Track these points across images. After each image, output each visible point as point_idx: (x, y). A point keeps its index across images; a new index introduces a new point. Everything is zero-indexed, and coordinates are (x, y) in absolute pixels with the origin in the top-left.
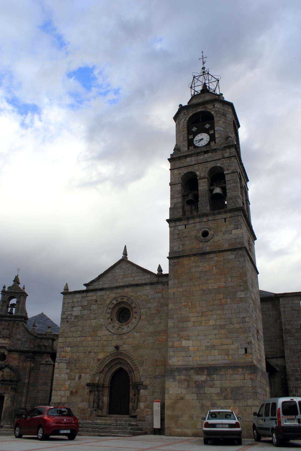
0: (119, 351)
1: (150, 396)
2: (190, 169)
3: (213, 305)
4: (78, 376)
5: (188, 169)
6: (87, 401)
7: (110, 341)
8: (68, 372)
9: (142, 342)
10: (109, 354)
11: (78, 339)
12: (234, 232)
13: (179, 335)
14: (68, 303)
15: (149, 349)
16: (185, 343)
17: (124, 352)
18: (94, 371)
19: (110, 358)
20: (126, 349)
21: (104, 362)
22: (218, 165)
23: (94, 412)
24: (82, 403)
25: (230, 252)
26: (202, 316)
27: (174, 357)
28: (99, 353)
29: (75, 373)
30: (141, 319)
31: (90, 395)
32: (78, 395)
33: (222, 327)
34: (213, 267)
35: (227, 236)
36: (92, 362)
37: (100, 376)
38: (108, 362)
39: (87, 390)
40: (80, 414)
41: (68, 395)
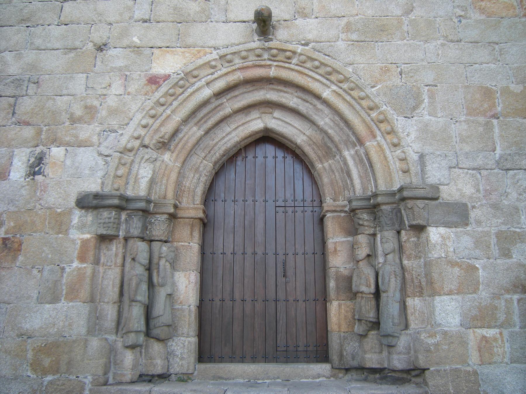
0: (272, 44)
1: (489, 258)
4: (25, 159)
6: (84, 293)
9: (399, 12)
10: (215, 55)
15: (439, 42)
17: (300, 49)
18: (130, 130)
19: (220, 73)
20: (310, 36)
21: (186, 94)
23: (129, 358)
24: (48, 306)
28: (155, 50)
29: (9, 146)
31: (97, 262)
32: (21, 258)
36: (117, 88)
37: (158, 164)
38: (207, 92)
39: (83, 233)
40: (34, 370)
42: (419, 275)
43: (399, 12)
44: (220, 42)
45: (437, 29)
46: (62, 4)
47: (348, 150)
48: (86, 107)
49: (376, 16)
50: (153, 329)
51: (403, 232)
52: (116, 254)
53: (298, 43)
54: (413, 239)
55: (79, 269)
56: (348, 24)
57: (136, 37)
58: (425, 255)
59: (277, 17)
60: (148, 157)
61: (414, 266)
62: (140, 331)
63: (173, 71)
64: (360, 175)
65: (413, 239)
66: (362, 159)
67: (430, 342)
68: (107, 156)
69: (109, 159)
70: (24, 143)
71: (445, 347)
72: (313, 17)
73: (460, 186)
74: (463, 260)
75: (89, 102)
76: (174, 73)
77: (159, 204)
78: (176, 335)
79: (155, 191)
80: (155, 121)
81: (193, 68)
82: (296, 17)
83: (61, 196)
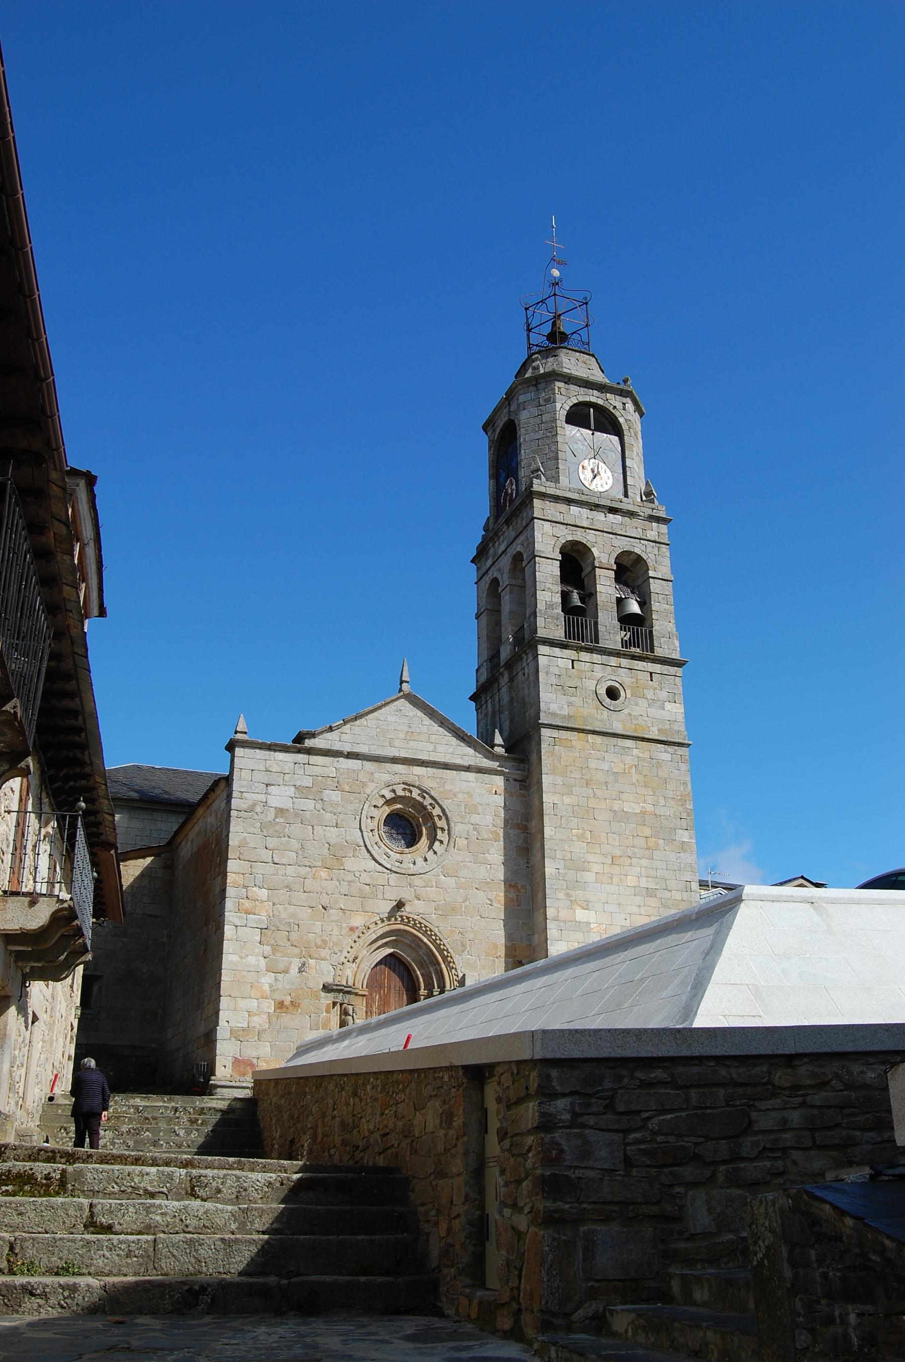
2: (579, 536)
3: (633, 847)
5: (575, 533)
7: (382, 887)
8: (265, 952)
11: (290, 870)
12: (668, 706)
13: (568, 895)
14: (252, 770)
16: (580, 914)
17: (416, 917)
22: (637, 551)
25: (663, 745)
26: (613, 863)
27: (561, 940)
29: (289, 957)
30: (456, 846)
33: (650, 893)
34: (631, 767)
35: (654, 712)
36: (336, 932)
41: (271, 1011)
43: (461, 901)
56: (438, 905)
70: (296, 956)
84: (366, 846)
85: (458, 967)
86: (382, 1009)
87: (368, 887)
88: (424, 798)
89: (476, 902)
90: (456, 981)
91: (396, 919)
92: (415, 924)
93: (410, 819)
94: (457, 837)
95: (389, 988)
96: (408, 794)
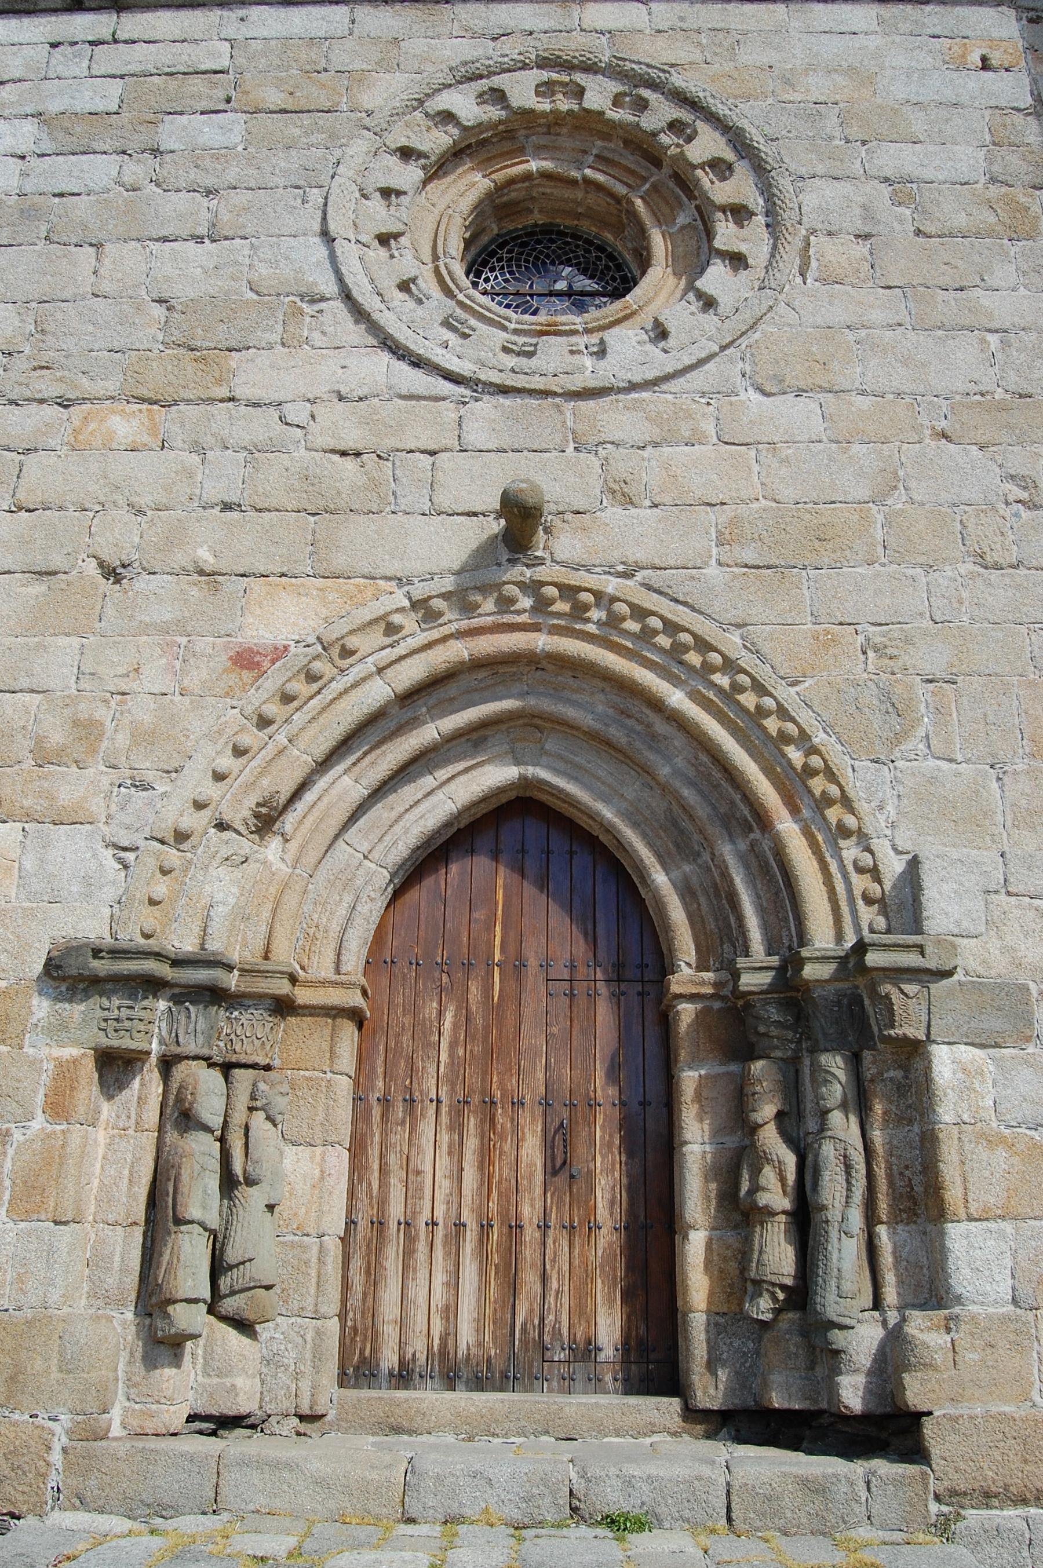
17: (611, 585)
20: (638, 554)
21: (328, 694)
30: (814, 264)
42: (907, 1167)
43: (864, 493)
44: (414, 566)
45: (960, 536)
46: (22, 457)
47: (732, 841)
48: (76, 723)
49: (805, 503)
50: (226, 1296)
51: (867, 1055)
52: (139, 1098)
53: (607, 569)
54: (892, 1074)
55: (48, 1136)
56: (735, 522)
57: (205, 548)
58: (922, 1115)
59: (557, 503)
60: (229, 853)
61: (895, 1142)
62: (196, 1301)
63: (297, 638)
64: (761, 905)
65: (892, 1074)
66: (767, 863)
67: (932, 1344)
68: (125, 849)
69: (130, 856)
71: (971, 1356)
72: (648, 503)
73: (1009, 940)
74: (1018, 1130)
75: (84, 710)
76: (298, 642)
77: (252, 971)
78: (284, 1313)
79: (244, 939)
80: (248, 762)
81: (346, 630)
82: (605, 504)
83: (8, 947)
84: (347, 297)
85: (876, 824)
86: (474, 1080)
87: (349, 463)
88: (642, 105)
89: (945, 497)
90: (869, 901)
91: (506, 603)
92: (614, 621)
93: (609, 236)
94: (814, 232)
95: (516, 967)
96: (565, 104)
